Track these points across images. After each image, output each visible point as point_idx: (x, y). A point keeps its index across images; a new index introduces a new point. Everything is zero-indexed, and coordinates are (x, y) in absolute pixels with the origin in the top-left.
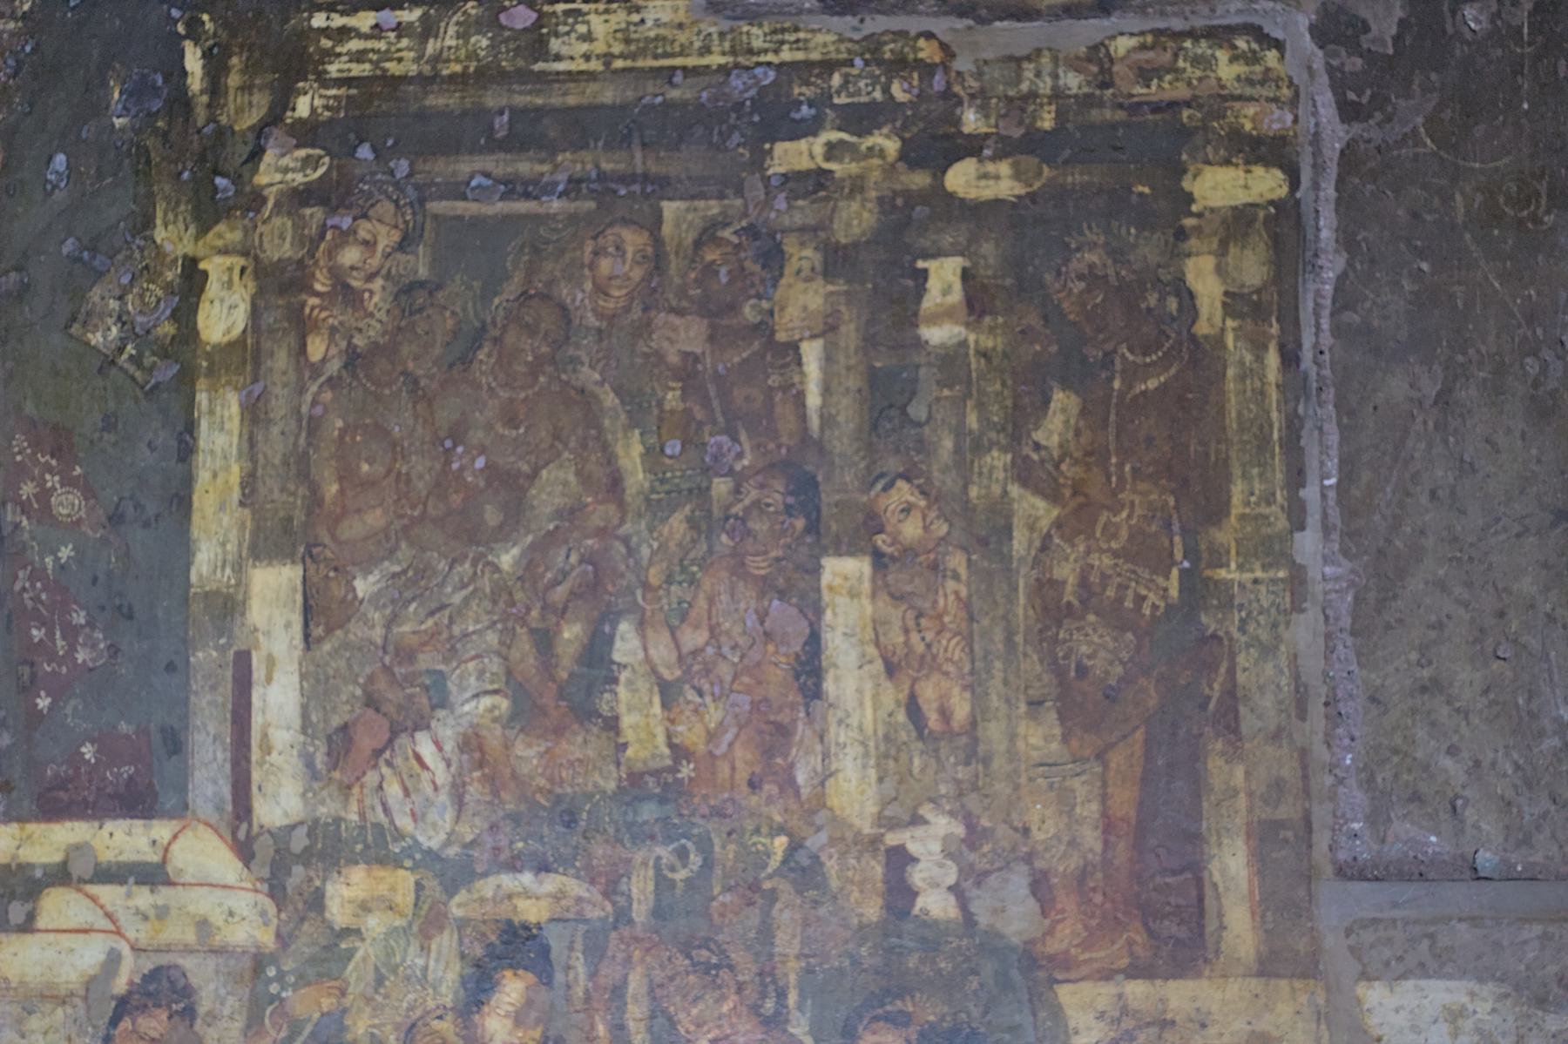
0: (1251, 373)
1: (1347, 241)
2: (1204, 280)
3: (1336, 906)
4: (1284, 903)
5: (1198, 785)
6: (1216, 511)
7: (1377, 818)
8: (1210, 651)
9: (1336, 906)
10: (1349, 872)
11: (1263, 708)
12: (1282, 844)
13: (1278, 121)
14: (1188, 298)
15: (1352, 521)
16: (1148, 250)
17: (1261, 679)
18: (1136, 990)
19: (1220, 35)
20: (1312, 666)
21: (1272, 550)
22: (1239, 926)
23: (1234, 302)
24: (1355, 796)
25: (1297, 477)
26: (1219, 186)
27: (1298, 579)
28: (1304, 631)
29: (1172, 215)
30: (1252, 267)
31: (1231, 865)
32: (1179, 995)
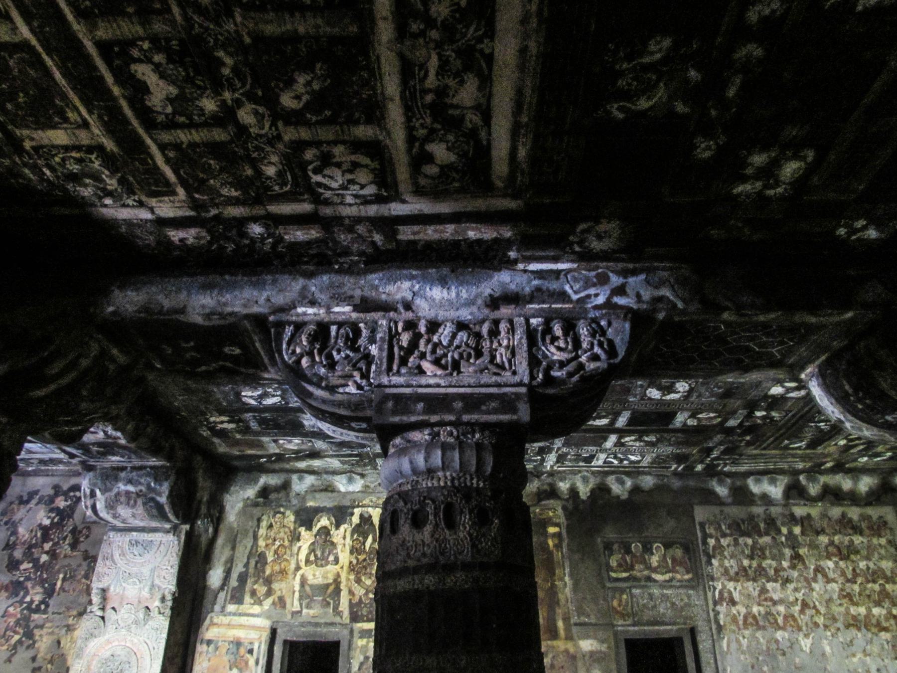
0: (558, 556)
1: (568, 537)
2: (550, 543)
3: (574, 630)
4: (568, 629)
5: (555, 613)
6: (554, 574)
7: (579, 617)
8: (556, 593)
9: (574, 630)
10: (576, 624)
11: (562, 602)
12: (566, 619)
13: (558, 521)
14: (548, 545)
15: (571, 575)
16: (542, 539)
17: (561, 596)
18: (549, 642)
19: (550, 509)
20: (569, 595)
21: (562, 579)
22: (562, 633)
23: (555, 546)
24: (575, 613)
25: (564, 570)
26: (552, 530)
27: (566, 584)
28: (567, 590)
29: (545, 534)
30: (556, 542)
31: (560, 624)
32: (555, 643)
